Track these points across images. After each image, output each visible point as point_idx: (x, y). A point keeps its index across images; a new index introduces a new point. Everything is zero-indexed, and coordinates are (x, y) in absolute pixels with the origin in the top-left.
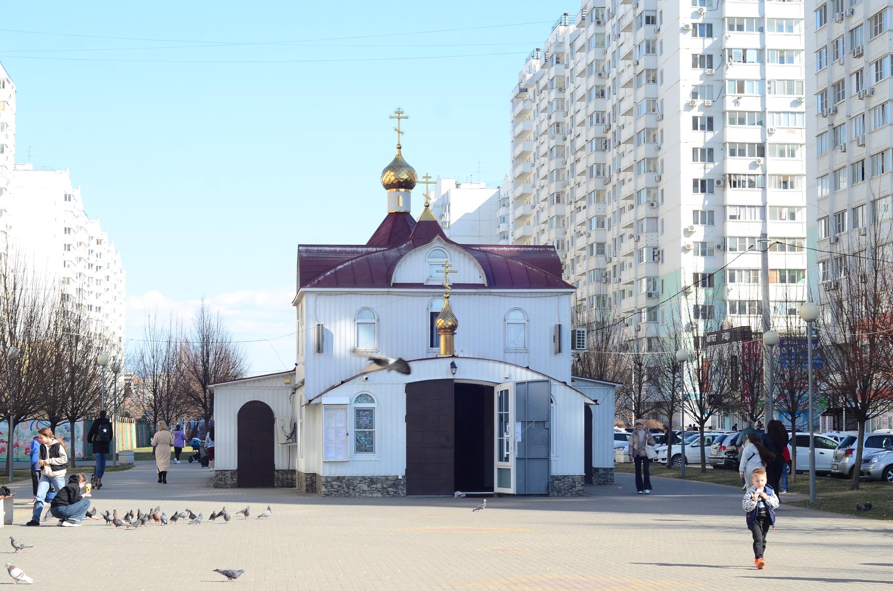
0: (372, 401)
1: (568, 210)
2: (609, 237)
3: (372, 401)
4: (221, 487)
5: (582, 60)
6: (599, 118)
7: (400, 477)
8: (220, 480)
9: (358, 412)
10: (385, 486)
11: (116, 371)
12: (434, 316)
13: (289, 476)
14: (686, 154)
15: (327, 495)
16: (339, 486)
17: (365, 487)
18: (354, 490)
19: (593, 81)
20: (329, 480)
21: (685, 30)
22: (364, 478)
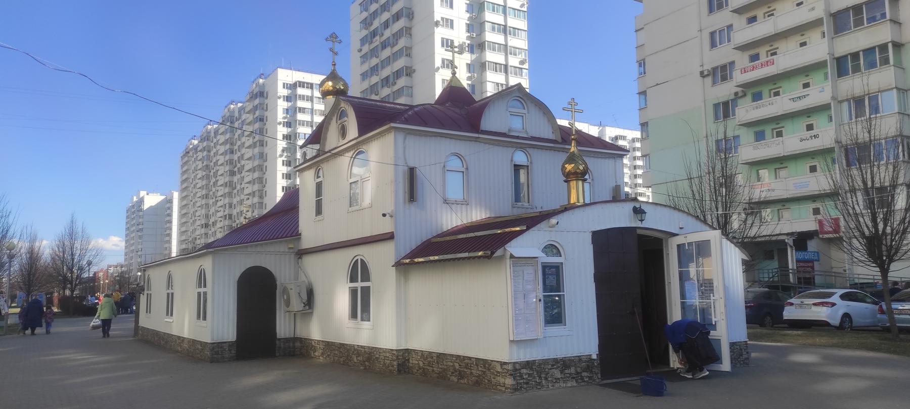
0: (559, 254)
1: (211, 202)
2: (235, 212)
3: (559, 254)
4: (218, 361)
5: (222, 139)
6: (231, 162)
7: (594, 357)
8: (217, 353)
9: (545, 267)
10: (579, 370)
11: (11, 257)
12: (517, 168)
13: (291, 345)
14: (279, 176)
15: (516, 390)
16: (530, 375)
17: (558, 375)
18: (546, 379)
19: (228, 146)
20: (518, 367)
21: (280, 123)
22: (556, 361)
